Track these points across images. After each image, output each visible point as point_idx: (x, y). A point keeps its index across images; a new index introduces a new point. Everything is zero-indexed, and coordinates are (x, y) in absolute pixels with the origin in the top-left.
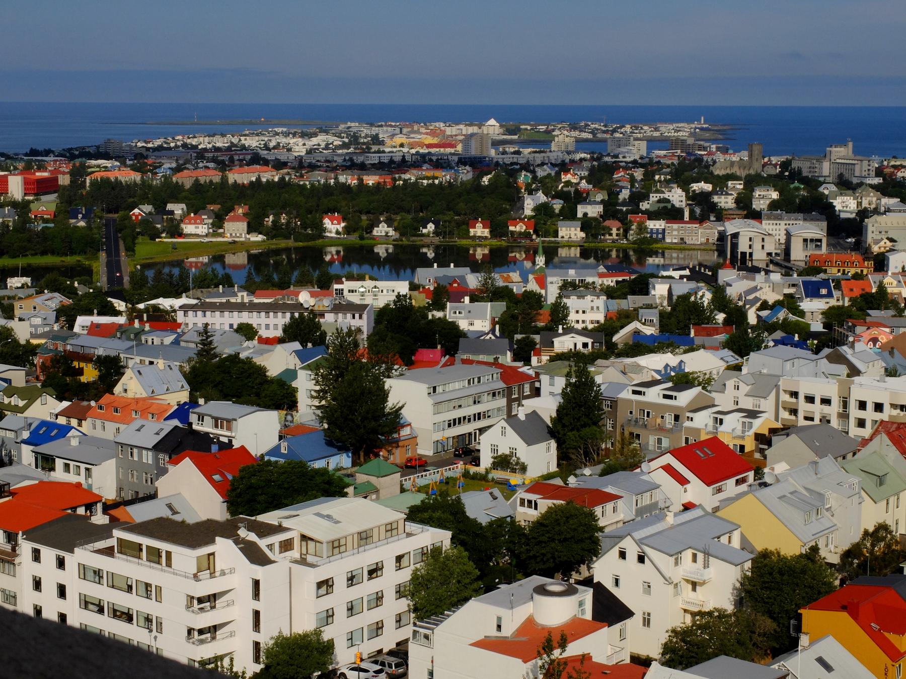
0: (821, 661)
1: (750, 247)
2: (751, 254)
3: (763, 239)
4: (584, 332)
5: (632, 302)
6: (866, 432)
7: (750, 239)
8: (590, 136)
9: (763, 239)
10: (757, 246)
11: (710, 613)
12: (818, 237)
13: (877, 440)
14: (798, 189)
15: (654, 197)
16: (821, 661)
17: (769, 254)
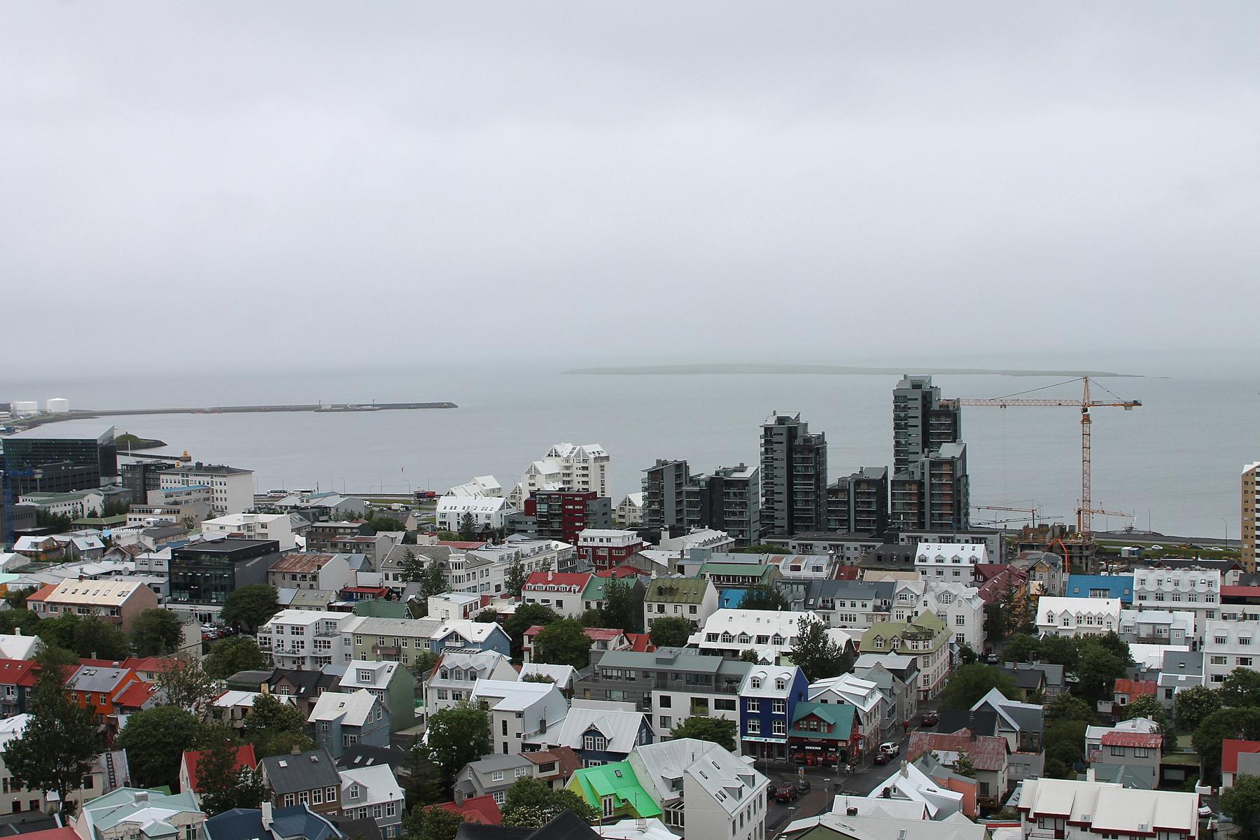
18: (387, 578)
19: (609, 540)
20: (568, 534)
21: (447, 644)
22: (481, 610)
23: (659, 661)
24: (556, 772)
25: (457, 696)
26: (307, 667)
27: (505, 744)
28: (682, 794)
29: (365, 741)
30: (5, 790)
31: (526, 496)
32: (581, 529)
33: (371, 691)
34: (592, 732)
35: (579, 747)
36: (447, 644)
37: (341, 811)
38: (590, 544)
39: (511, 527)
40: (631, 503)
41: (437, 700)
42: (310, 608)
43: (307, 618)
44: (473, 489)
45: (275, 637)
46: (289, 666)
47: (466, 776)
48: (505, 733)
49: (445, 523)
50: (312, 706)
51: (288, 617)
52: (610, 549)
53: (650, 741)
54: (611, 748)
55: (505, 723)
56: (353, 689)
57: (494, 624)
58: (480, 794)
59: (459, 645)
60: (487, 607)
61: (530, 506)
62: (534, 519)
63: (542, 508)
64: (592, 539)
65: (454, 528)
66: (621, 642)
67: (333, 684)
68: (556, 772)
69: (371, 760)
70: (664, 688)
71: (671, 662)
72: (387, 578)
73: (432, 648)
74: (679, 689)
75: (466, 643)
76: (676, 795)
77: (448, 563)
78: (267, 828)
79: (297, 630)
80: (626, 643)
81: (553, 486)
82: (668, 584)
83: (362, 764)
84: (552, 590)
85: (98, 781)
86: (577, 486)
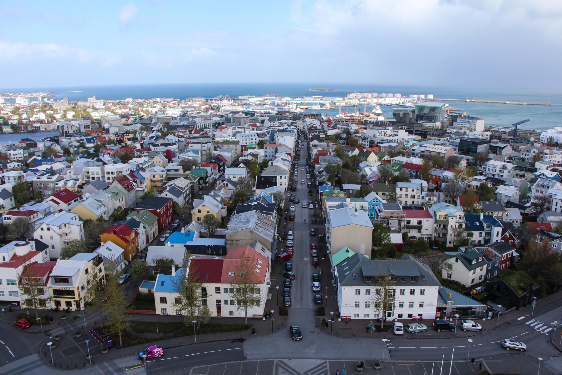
0: (107, 248)
1: (68, 129)
2: (68, 131)
3: (72, 127)
4: (18, 161)
5: (32, 150)
6: (111, 181)
7: (68, 127)
8: (9, 98)
9: (72, 127)
10: (70, 129)
11: (73, 241)
12: (88, 125)
13: (114, 182)
14: (80, 111)
15: (35, 116)
16: (107, 248)
17: (74, 131)
18: (523, 155)
21: (540, 176)
22: (552, 168)
26: (497, 177)
27: (556, 209)
29: (511, 200)
30: (411, 198)
33: (515, 187)
36: (540, 176)
37: (502, 219)
41: (535, 192)
44: (553, 131)
46: (490, 176)
47: (542, 216)
48: (556, 205)
49: (543, 140)
50: (497, 188)
51: (492, 162)
55: (557, 203)
56: (509, 186)
57: (557, 173)
58: (545, 222)
59: (544, 177)
60: (554, 167)
65: (546, 142)
67: (503, 183)
69: (512, 207)
72: (523, 155)
73: (535, 177)
75: (547, 177)
77: (543, 153)
78: (481, 220)
79: (495, 166)
83: (510, 207)
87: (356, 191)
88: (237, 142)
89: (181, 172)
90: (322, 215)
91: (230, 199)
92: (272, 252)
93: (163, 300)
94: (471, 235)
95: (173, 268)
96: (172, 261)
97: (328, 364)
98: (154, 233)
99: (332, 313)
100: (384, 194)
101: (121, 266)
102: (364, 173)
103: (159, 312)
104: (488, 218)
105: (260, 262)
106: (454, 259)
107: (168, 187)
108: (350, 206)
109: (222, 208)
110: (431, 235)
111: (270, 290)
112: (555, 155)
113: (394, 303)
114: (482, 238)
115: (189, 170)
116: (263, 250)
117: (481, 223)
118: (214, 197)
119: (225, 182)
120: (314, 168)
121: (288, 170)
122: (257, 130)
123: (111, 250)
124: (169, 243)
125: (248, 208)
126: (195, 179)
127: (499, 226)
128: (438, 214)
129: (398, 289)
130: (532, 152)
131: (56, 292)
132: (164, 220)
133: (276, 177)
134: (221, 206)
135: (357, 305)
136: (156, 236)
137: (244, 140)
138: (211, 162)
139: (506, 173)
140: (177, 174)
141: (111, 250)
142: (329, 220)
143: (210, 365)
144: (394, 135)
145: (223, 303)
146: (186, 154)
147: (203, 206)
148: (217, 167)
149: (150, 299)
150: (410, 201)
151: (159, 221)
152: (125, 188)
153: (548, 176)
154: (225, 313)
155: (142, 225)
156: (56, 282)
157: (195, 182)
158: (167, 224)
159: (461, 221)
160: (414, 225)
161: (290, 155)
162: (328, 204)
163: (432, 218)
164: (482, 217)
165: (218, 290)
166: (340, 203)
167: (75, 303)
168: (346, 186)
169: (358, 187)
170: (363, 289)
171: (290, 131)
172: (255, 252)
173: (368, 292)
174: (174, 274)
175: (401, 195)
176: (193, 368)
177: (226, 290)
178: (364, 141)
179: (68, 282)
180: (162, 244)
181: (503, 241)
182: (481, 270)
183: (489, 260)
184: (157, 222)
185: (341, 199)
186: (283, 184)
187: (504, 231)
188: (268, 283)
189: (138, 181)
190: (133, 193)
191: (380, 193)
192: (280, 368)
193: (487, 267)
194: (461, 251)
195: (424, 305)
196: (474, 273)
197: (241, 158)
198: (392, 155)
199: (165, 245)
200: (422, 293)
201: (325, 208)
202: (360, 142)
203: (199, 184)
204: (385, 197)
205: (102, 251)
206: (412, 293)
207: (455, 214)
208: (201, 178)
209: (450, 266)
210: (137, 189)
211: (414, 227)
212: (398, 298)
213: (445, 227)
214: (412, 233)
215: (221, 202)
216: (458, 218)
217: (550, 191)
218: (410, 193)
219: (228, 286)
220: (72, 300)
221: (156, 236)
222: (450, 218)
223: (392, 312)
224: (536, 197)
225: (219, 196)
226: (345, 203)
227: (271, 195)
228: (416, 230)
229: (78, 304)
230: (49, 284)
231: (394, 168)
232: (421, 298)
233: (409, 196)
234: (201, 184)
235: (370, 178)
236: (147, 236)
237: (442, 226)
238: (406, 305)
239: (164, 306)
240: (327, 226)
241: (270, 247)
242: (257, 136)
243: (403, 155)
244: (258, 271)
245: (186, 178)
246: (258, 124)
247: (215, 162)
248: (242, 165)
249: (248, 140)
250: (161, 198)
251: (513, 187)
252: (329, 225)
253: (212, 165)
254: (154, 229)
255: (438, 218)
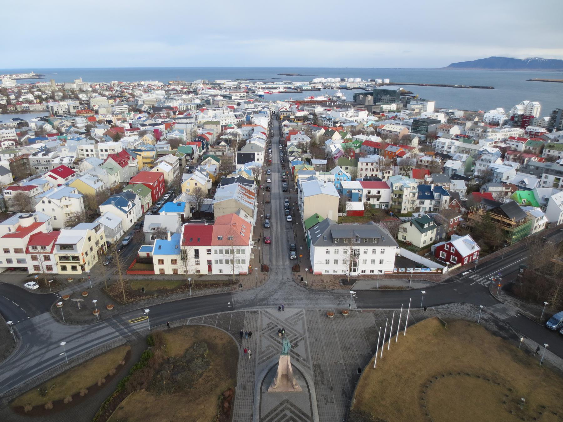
0: (107, 218)
6: (105, 158)
19: (536, 130)
20: (523, 126)
22: (494, 145)
23: (546, 166)
24: (510, 190)
25: (484, 166)
26: (445, 153)
28: (547, 203)
29: (457, 173)
31: (512, 115)
32: (527, 126)
33: (461, 161)
34: (523, 182)
35: (517, 185)
38: (529, 130)
39: (506, 123)
40: (544, 120)
42: (447, 138)
43: (447, 142)
45: (437, 144)
46: (439, 152)
47: (484, 186)
50: (445, 163)
51: (441, 140)
52: (536, 132)
53: (539, 187)
54: (527, 187)
56: (456, 160)
57: (498, 149)
61: (513, 118)
62: (512, 121)
63: (516, 119)
64: (530, 129)
66: (535, 159)
67: (450, 158)
68: (510, 190)
70: (547, 173)
71: (551, 166)
74: (552, 174)
75: (489, 153)
76: (545, 203)
79: (443, 143)
80: (536, 159)
81: (520, 112)
82: (552, 145)
83: (456, 179)
84: (516, 142)
85: (392, 172)
86: (528, 113)
87: (323, 165)
88: (218, 123)
89: (170, 149)
90: (294, 186)
91: (215, 172)
92: (253, 217)
93: (161, 262)
94: (422, 203)
95: (169, 234)
96: (165, 228)
97: (304, 311)
98: (148, 203)
99: (307, 269)
100: (347, 168)
101: (120, 233)
102: (330, 151)
103: (157, 272)
104: (438, 189)
105: (244, 227)
106: (409, 223)
107: (159, 163)
108: (319, 179)
109: (208, 181)
110: (388, 203)
111: (253, 251)
112: (496, 133)
113: (358, 261)
114: (431, 206)
115: (177, 148)
116: (246, 216)
117: (431, 193)
118: (201, 171)
119: (210, 158)
120: (286, 145)
121: (264, 147)
122: (234, 112)
123: (110, 220)
124: (164, 212)
125: (232, 181)
126: (182, 155)
127: (448, 195)
128: (395, 185)
129: (362, 249)
130: (476, 130)
131: (61, 258)
132: (157, 192)
133: (254, 154)
134: (207, 179)
135: (327, 262)
136: (150, 206)
137: (224, 120)
138: (195, 141)
139: (452, 150)
140: (166, 151)
141: (110, 220)
142: (301, 191)
143: (204, 316)
144: (355, 116)
145: (213, 263)
146: (173, 134)
147: (192, 179)
148: (201, 145)
149: (149, 261)
150: (369, 174)
151: (152, 193)
152: (119, 164)
153: (490, 152)
154: (215, 271)
155: (137, 197)
156: (61, 249)
157: (183, 158)
158: (160, 195)
159: (415, 191)
160: (374, 194)
161: (265, 134)
162: (301, 177)
163: (389, 188)
164: (432, 188)
165: (209, 251)
166: (310, 176)
167: (80, 267)
168: (314, 161)
169: (325, 162)
170: (332, 249)
171: (264, 113)
172: (240, 218)
173: (337, 252)
174: (169, 238)
175: (362, 170)
176: (189, 319)
177: (216, 252)
178: (328, 122)
179: (73, 249)
180: (156, 213)
181: (450, 208)
182: (432, 233)
183: (439, 224)
184: (150, 194)
185: (310, 173)
186: (260, 160)
187: (452, 199)
188: (251, 245)
189: (131, 157)
190: (126, 168)
191: (344, 167)
192: (264, 316)
193: (437, 230)
194: (413, 216)
195: (384, 262)
196: (426, 235)
197: (222, 137)
198: (354, 134)
199: (159, 214)
200: (383, 252)
201: (298, 180)
202: (326, 122)
203: (186, 160)
204: (348, 171)
205: (101, 220)
206: (374, 252)
207: (409, 185)
208: (188, 155)
209: (405, 230)
210: (130, 165)
211: (374, 196)
212: (362, 256)
213: (400, 196)
214: (373, 201)
215: (206, 176)
216: (412, 188)
217: (492, 165)
218: (370, 166)
219: (218, 248)
220: (77, 265)
221: (150, 206)
222: (405, 189)
223: (356, 268)
224: (479, 171)
225: (205, 170)
226: (314, 175)
227: (250, 169)
228: (375, 199)
229: (83, 267)
230: (55, 251)
231: (356, 145)
232: (382, 257)
233: (369, 170)
234: (188, 160)
235: (336, 154)
236: (142, 206)
237: (397, 196)
238: (369, 262)
239: (161, 266)
240: (299, 195)
241: (251, 215)
242: (234, 117)
243: (363, 134)
244: (243, 235)
245: (174, 155)
246: (235, 107)
247: (199, 141)
248: (223, 143)
249: (227, 120)
250: (152, 172)
251: (459, 161)
252: (301, 195)
253: (197, 143)
254: (148, 200)
255: (394, 188)
